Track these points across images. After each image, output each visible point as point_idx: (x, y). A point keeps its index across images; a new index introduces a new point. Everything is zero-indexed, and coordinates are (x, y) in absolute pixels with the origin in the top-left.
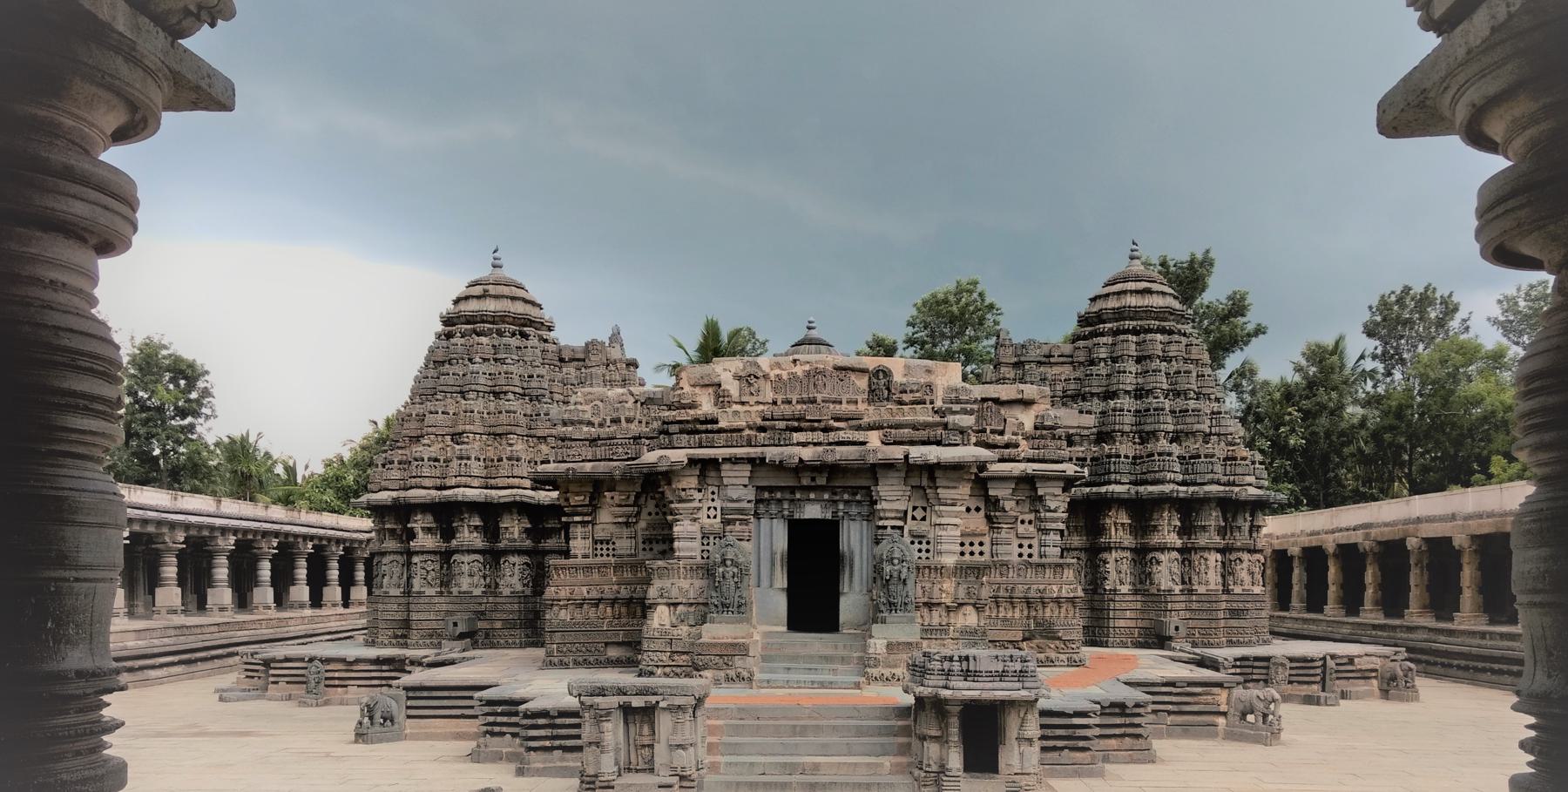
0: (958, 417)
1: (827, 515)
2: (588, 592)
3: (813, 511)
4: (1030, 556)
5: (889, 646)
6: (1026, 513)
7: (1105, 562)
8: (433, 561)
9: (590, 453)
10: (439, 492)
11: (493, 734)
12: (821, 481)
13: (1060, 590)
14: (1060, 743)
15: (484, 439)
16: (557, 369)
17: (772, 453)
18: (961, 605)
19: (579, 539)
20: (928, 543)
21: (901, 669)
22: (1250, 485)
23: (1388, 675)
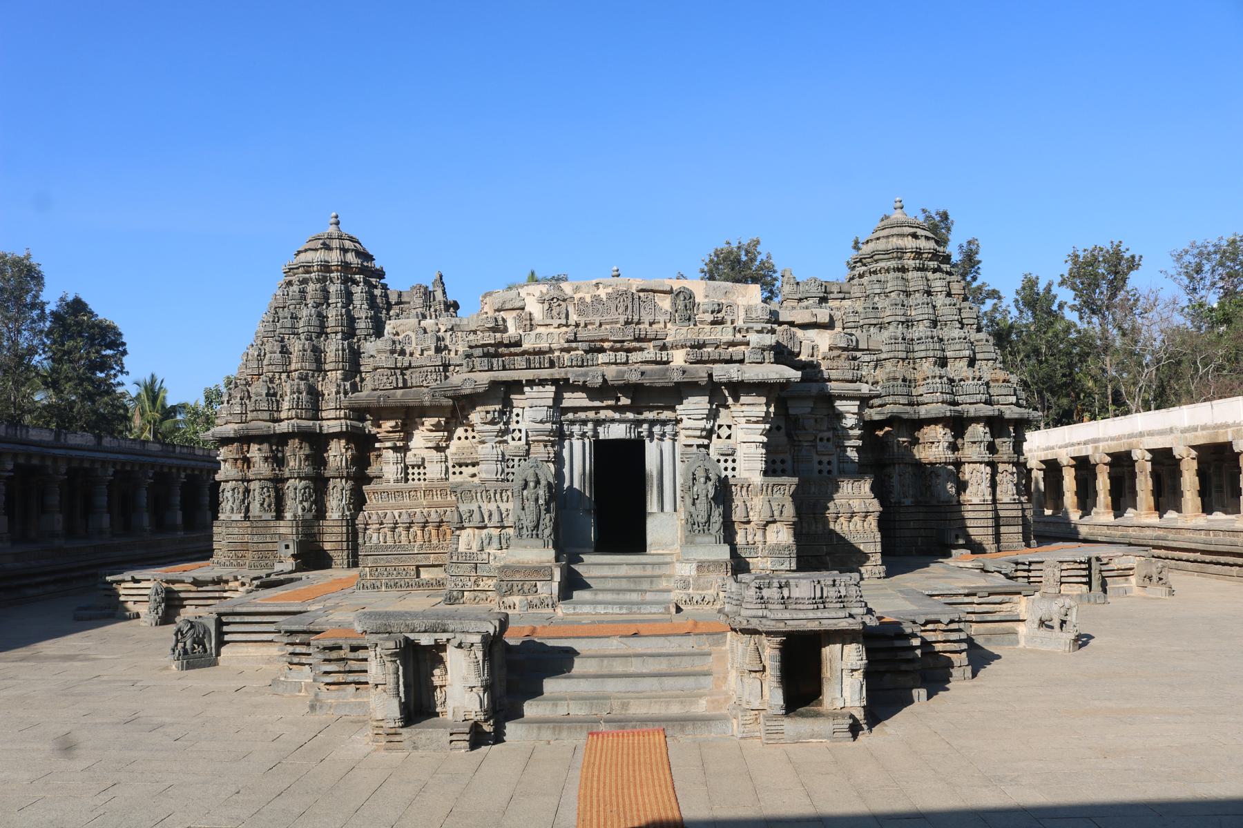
0: (761, 335)
1: (633, 435)
2: (399, 517)
3: (617, 431)
4: (829, 472)
5: (701, 566)
6: (824, 431)
7: (890, 477)
8: (268, 488)
9: (400, 381)
10: (276, 424)
11: (291, 663)
12: (625, 401)
13: (860, 505)
14: (882, 668)
15: (316, 375)
16: (384, 312)
17: (573, 375)
18: (768, 523)
19: (391, 463)
20: (734, 461)
21: (712, 590)
22: (1012, 404)
23: (1144, 574)
